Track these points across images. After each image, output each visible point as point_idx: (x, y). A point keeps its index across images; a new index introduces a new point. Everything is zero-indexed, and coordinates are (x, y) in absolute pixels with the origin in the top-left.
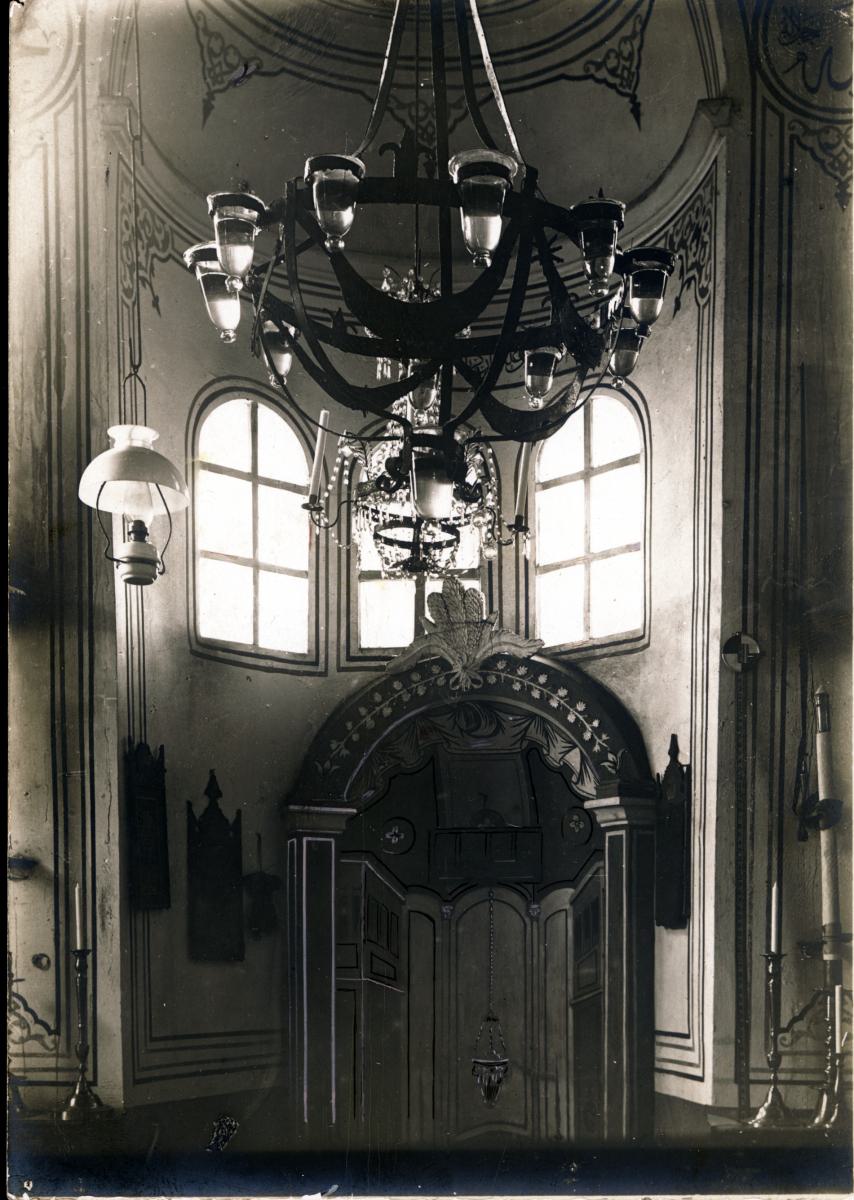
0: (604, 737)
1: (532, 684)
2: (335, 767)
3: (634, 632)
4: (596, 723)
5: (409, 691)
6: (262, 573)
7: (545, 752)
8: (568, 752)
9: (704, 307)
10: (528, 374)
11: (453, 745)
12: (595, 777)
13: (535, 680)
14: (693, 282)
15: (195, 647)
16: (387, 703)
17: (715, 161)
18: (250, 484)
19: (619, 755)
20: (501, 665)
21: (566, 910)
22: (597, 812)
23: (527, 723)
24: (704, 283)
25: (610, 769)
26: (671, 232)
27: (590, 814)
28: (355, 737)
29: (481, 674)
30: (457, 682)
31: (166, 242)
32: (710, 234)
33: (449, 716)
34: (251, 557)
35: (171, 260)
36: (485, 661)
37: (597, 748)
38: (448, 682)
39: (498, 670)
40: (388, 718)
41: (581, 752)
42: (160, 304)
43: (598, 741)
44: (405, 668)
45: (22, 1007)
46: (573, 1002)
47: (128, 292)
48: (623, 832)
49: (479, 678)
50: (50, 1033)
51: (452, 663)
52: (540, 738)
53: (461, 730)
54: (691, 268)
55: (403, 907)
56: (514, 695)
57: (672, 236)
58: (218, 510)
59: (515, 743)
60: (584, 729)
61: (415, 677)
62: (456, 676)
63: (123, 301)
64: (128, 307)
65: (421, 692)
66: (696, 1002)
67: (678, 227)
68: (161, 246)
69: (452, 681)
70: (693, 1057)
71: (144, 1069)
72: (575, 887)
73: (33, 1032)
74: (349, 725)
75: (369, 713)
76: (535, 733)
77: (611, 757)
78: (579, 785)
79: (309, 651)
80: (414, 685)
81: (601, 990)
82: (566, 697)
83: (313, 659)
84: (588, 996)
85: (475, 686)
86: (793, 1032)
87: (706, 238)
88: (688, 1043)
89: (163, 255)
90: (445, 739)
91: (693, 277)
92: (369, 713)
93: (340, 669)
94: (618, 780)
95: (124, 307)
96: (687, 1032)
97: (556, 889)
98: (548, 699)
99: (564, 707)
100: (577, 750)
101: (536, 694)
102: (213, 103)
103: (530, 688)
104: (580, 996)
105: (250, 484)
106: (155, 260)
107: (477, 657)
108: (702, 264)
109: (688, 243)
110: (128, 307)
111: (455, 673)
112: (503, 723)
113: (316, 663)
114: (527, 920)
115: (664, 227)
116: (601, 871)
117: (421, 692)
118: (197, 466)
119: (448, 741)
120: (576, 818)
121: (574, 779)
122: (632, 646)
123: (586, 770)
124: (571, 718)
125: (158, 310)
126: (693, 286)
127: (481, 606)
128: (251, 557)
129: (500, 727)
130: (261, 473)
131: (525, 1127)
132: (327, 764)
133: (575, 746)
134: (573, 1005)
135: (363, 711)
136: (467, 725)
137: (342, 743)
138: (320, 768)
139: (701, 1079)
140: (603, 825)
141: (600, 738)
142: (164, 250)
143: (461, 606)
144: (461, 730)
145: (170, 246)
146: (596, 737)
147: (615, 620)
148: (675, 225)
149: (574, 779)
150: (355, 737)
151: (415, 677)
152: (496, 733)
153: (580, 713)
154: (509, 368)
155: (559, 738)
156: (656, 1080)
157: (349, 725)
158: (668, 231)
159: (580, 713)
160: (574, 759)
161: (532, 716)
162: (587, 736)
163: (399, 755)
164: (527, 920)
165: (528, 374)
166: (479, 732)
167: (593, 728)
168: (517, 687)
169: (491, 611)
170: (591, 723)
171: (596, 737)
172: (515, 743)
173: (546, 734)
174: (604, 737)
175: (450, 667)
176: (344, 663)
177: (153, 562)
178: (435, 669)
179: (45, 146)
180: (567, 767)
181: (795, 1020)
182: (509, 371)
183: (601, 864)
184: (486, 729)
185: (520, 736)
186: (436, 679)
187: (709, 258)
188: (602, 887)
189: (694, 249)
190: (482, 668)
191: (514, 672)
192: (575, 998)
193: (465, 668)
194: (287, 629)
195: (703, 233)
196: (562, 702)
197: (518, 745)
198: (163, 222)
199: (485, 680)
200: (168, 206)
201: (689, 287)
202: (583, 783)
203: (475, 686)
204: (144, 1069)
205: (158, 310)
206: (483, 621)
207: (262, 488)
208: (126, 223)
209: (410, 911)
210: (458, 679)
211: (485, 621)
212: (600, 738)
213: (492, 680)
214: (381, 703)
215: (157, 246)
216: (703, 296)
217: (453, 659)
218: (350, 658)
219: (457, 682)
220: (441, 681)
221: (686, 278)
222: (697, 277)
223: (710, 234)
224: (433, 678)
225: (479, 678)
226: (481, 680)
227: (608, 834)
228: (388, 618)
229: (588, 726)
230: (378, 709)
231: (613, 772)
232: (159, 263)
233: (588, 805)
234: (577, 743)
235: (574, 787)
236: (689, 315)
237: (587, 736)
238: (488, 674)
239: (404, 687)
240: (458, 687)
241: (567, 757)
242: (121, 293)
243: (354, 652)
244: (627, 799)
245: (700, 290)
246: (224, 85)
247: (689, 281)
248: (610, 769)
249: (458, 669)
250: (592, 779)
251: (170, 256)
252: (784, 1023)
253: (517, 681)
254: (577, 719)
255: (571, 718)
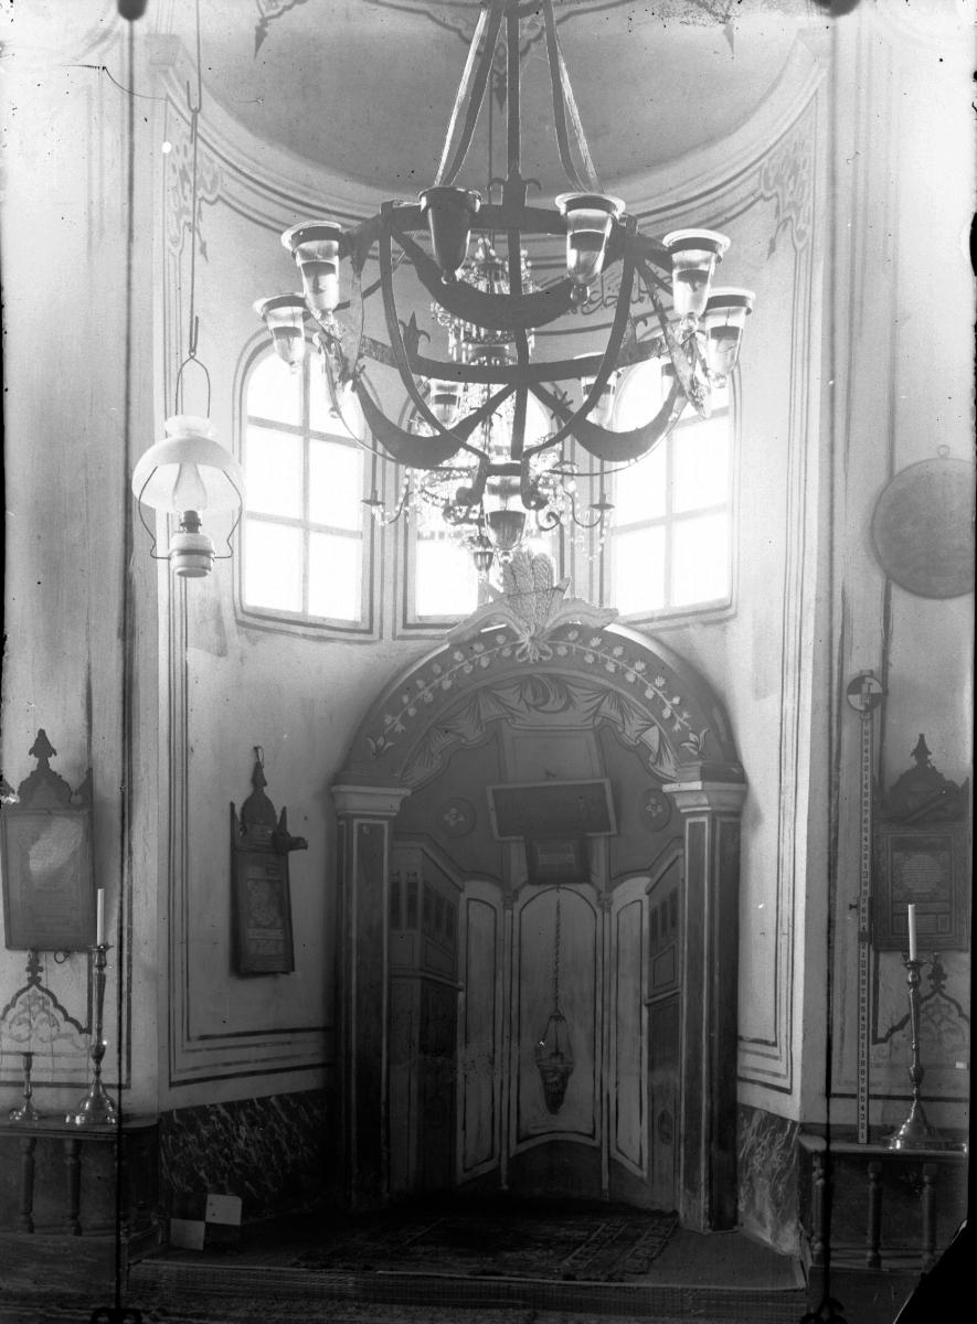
0: (685, 715)
1: (606, 656)
2: (389, 744)
3: (721, 601)
4: (676, 700)
5: (470, 663)
6: (313, 536)
7: (620, 729)
8: (646, 729)
9: (802, 251)
10: (572, 247)
11: (518, 721)
12: (675, 758)
13: (609, 652)
14: (790, 223)
15: (240, 616)
16: (447, 675)
17: (816, 93)
18: (301, 438)
19: (702, 735)
20: (573, 635)
21: (641, 901)
22: (676, 796)
23: (600, 699)
24: (801, 225)
25: (692, 750)
26: (766, 166)
27: (669, 799)
28: (412, 712)
29: (549, 645)
30: (524, 653)
31: (214, 183)
32: (808, 172)
33: (515, 688)
34: (302, 517)
35: (220, 204)
36: (553, 631)
37: (677, 727)
38: (514, 653)
39: (569, 641)
40: (448, 691)
41: (660, 730)
42: (208, 250)
43: (679, 719)
44: (467, 637)
45: (51, 1003)
46: (648, 1001)
47: (175, 242)
48: (705, 819)
49: (547, 648)
50: (81, 1031)
51: (518, 632)
52: (614, 714)
53: (528, 705)
54: (788, 208)
55: (462, 895)
56: (585, 668)
57: (766, 173)
58: (267, 470)
59: (588, 719)
60: (664, 706)
61: (478, 647)
62: (523, 647)
63: (169, 250)
64: (173, 255)
65: (484, 663)
66: (783, 1005)
67: (774, 161)
68: (209, 187)
69: (518, 653)
70: (781, 1067)
71: (181, 1071)
72: (652, 876)
73: (62, 1031)
74: (405, 699)
75: (427, 685)
76: (608, 709)
77: (692, 737)
78: (657, 766)
79: (363, 618)
80: (477, 656)
81: (679, 990)
82: (643, 671)
83: (366, 626)
84: (665, 995)
85: (544, 658)
86: (891, 1043)
87: (805, 177)
88: (774, 1051)
89: (211, 198)
90: (511, 714)
91: (790, 218)
92: (427, 685)
93: (395, 637)
94: (700, 763)
95: (171, 257)
96: (772, 1039)
97: (633, 877)
98: (623, 674)
99: (641, 682)
100: (655, 729)
101: (611, 668)
102: (267, 29)
103: (605, 661)
104: (655, 996)
105: (301, 438)
106: (203, 203)
107: (547, 626)
108: (799, 204)
109: (786, 178)
110: (173, 255)
111: (522, 644)
112: (574, 697)
113: (370, 631)
114: (598, 911)
115: (760, 158)
116: (681, 860)
117: (484, 663)
118: (244, 419)
119: (513, 716)
120: (653, 801)
121: (652, 759)
122: (717, 616)
123: (666, 750)
124: (649, 694)
125: (206, 257)
126: (789, 227)
127: (551, 572)
128: (302, 517)
129: (570, 702)
130: (314, 426)
131: (592, 1136)
132: (381, 741)
133: (653, 724)
134: (648, 1005)
135: (420, 683)
136: (534, 699)
137: (398, 718)
138: (373, 746)
139: (788, 1091)
140: (683, 811)
141: (681, 716)
142: (210, 193)
143: (530, 572)
144: (528, 705)
145: (219, 186)
146: (676, 715)
147: (701, 587)
148: (770, 159)
149: (652, 759)
150: (412, 712)
151: (478, 647)
152: (565, 708)
153: (659, 688)
154: (585, 309)
155: (635, 715)
156: (739, 1088)
157: (405, 699)
158: (763, 164)
159: (659, 688)
160: (652, 737)
161: (605, 691)
162: (667, 713)
163: (458, 731)
164: (598, 911)
165: (572, 247)
166: (548, 707)
167: (673, 705)
168: (590, 659)
169: (562, 576)
170: (670, 699)
171: (676, 715)
172: (588, 719)
173: (622, 711)
174: (685, 715)
175: (516, 637)
176: (400, 631)
177: (206, 553)
178: (500, 639)
179: (90, 87)
180: (644, 746)
181: (893, 1030)
182: (584, 314)
183: (681, 852)
184: (555, 703)
185: (592, 711)
186: (501, 650)
187: (808, 199)
188: (682, 876)
189: (791, 188)
190: (552, 638)
191: (586, 642)
192: (650, 997)
193: (532, 639)
194: (340, 601)
195: (801, 171)
196: (639, 676)
197: (590, 721)
198: (212, 161)
199: (555, 651)
200: (228, 153)
201: (785, 227)
202: (661, 763)
203: (544, 658)
204: (181, 1071)
205: (206, 257)
206: (553, 588)
207: (314, 444)
208: (174, 167)
209: (469, 899)
210: (525, 650)
211: (557, 588)
212: (681, 716)
213: (562, 651)
214: (440, 675)
215: (205, 187)
216: (800, 239)
217: (521, 630)
218: (406, 626)
219: (524, 653)
220: (507, 653)
221: (781, 219)
222: (794, 216)
223: (808, 172)
224: (497, 649)
225: (547, 648)
226: (551, 651)
227: (689, 821)
228: (450, 584)
229: (667, 702)
230: (437, 681)
231: (696, 753)
232: (207, 206)
233: (667, 788)
234: (655, 721)
235: (652, 768)
236: (784, 260)
237: (667, 713)
238: (557, 645)
239: (466, 657)
240: (525, 659)
241: (644, 736)
242: (168, 243)
243: (410, 620)
244: (708, 784)
245: (797, 233)
246: (280, 9)
247: (785, 221)
248: (692, 750)
249: (525, 639)
250: (672, 759)
251: (219, 198)
252: (882, 1033)
253: (590, 653)
254: (656, 695)
255: (649, 694)
